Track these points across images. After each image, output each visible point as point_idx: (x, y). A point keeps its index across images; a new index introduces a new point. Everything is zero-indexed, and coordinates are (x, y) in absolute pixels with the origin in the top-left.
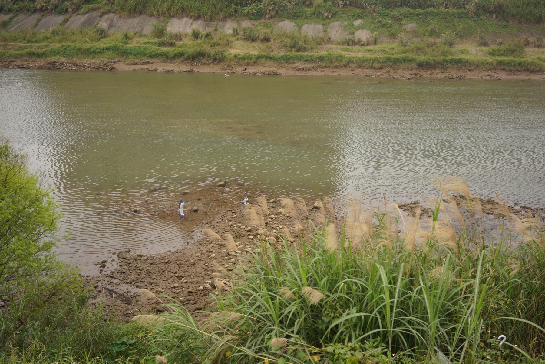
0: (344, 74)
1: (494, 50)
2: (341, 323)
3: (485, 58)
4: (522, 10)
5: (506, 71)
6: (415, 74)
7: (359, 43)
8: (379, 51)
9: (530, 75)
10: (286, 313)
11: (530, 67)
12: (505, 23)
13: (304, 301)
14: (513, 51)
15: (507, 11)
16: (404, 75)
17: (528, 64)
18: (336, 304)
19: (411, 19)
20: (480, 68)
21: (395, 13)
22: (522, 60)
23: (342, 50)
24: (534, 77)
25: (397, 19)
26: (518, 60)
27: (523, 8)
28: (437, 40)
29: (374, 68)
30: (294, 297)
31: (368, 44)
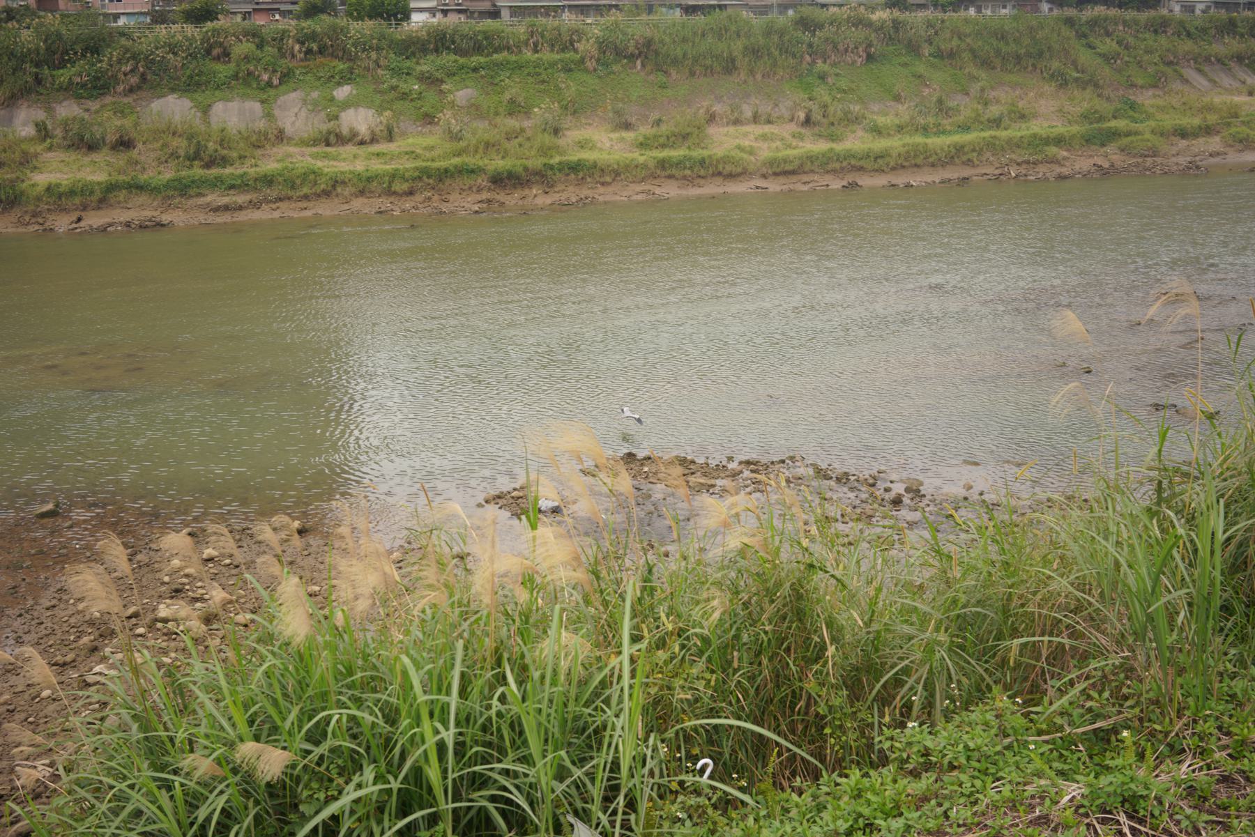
0: (328, 213)
1: (646, 138)
2: (343, 812)
3: (630, 156)
6: (489, 201)
7: (352, 138)
8: (400, 153)
9: (726, 183)
10: (200, 820)
11: (724, 168)
12: (661, 78)
13: (248, 778)
14: (685, 137)
15: (663, 52)
16: (464, 204)
17: (718, 161)
18: (327, 769)
19: (464, 80)
20: (623, 176)
21: (425, 68)
22: (706, 153)
23: (315, 156)
25: (431, 80)
26: (697, 153)
27: (694, 43)
28: (526, 124)
29: (395, 193)
30: (219, 772)
31: (374, 140)
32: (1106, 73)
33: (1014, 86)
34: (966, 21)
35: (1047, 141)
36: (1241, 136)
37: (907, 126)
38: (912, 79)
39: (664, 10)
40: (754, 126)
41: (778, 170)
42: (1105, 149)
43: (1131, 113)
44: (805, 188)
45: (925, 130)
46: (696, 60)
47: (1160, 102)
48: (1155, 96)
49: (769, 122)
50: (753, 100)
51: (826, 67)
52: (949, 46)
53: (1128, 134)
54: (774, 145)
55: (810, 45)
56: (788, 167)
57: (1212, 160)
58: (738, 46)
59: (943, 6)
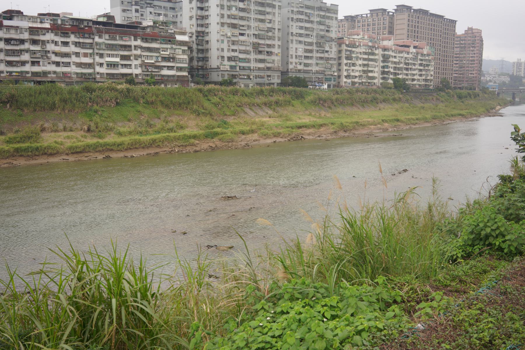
1: (10, 138)
4: (35, 98)
5: (25, 157)
9: (48, 158)
11: (48, 151)
12: (19, 112)
14: (29, 138)
17: (45, 148)
22: (39, 145)
24: (52, 160)
26: (35, 145)
32: (214, 110)
33: (179, 115)
34: (158, 89)
35: (190, 137)
36: (265, 133)
37: (133, 132)
38: (136, 112)
39: (26, 83)
40: (64, 132)
41: (73, 151)
42: (213, 140)
43: (225, 125)
44: (86, 159)
45: (141, 133)
46: (36, 104)
47: (236, 121)
48: (234, 119)
49: (71, 131)
50: (64, 121)
51: (98, 108)
52: (151, 99)
53: (222, 134)
54: (73, 141)
55: (90, 98)
56: (78, 150)
57: (254, 143)
58: (57, 99)
59: (150, 83)
